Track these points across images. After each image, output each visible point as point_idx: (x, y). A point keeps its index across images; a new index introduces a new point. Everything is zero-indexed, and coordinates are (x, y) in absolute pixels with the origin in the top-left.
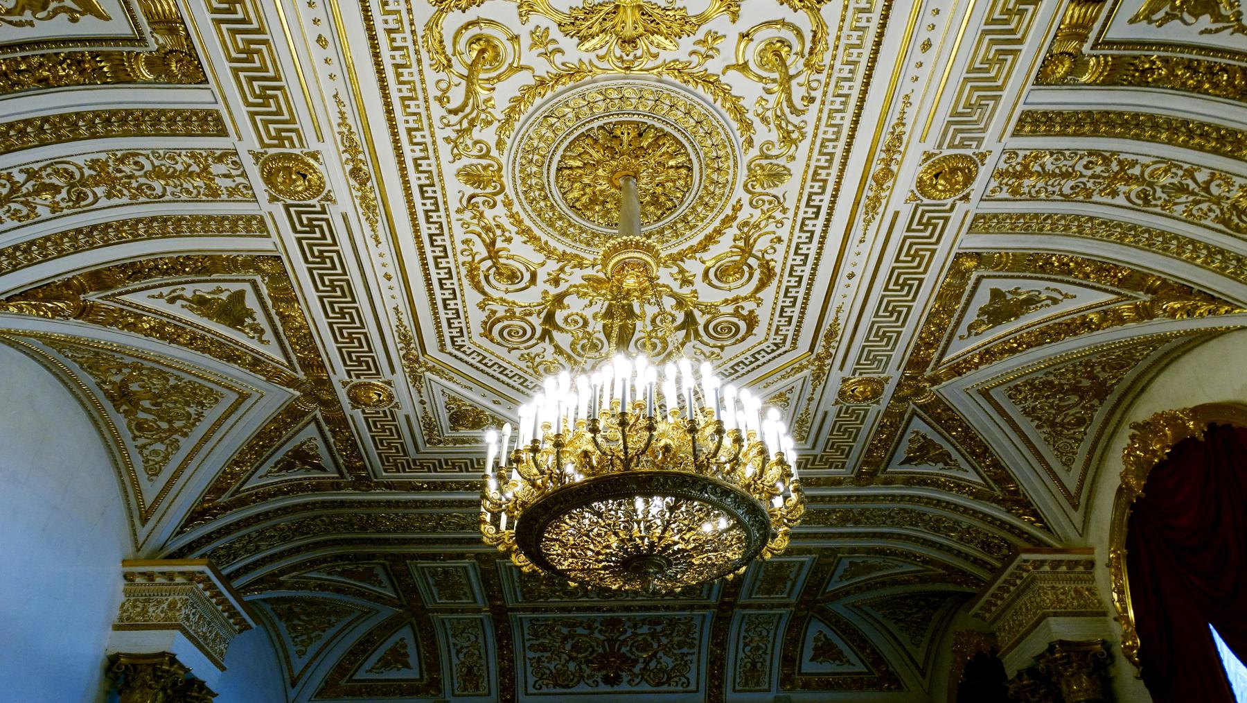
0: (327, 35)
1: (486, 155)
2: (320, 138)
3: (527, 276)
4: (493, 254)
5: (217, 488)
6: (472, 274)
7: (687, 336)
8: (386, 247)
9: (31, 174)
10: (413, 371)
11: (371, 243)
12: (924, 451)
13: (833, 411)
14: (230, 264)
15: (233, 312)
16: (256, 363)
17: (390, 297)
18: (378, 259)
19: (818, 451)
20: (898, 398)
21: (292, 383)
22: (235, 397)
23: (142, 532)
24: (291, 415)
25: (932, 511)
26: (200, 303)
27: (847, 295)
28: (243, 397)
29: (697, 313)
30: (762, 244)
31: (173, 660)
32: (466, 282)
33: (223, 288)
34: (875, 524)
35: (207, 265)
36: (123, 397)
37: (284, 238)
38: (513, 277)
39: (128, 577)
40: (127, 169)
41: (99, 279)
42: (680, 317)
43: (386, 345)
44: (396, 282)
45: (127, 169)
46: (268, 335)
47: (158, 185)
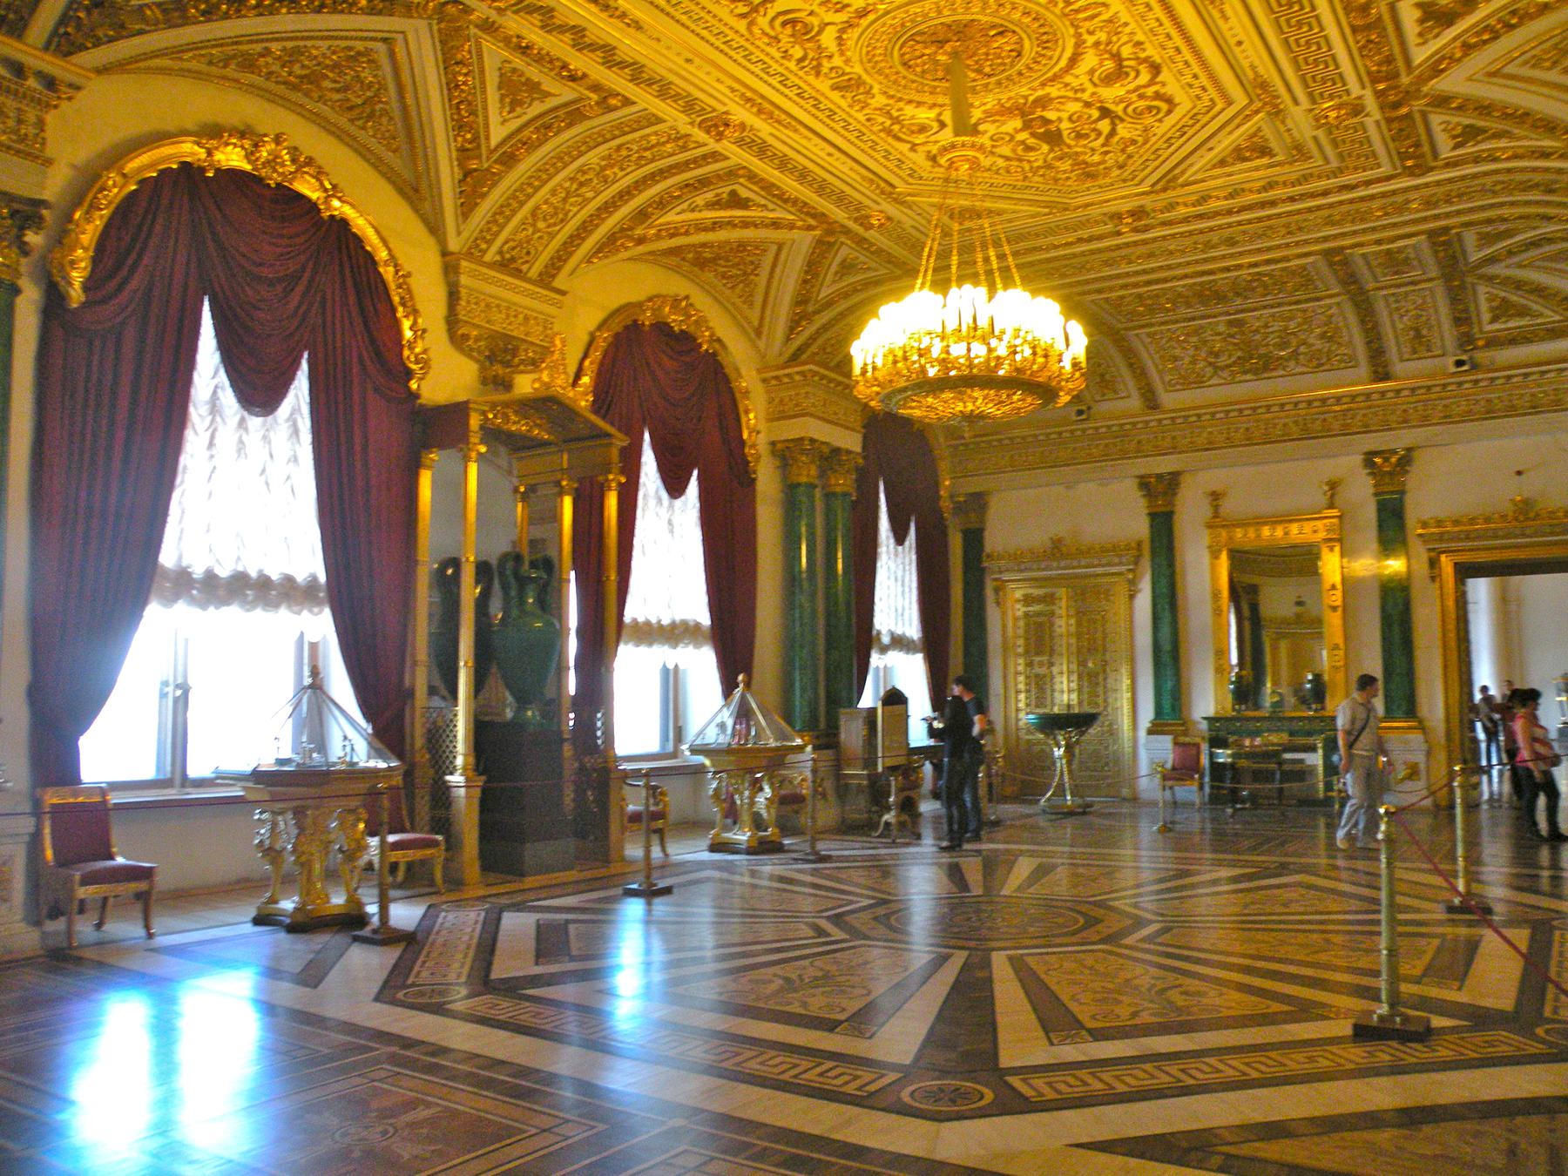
0: (690, 56)
1: (844, 74)
2: (724, 104)
3: (935, 125)
4: (896, 120)
5: (801, 300)
6: (889, 132)
7: (1114, 125)
8: (816, 140)
9: (572, 179)
10: (895, 200)
11: (804, 142)
12: (1471, 134)
13: (1320, 133)
14: (720, 177)
15: (736, 201)
16: (775, 224)
17: (843, 166)
18: (818, 149)
19: (1335, 164)
20: (1388, 105)
21: (810, 228)
22: (775, 247)
23: (762, 344)
24: (823, 248)
25: (1537, 178)
26: (711, 205)
27: (1252, 55)
28: (780, 246)
29: (1112, 107)
30: (1126, 51)
31: (812, 441)
32: (890, 140)
33: (725, 191)
34: (1471, 199)
35: (704, 182)
36: (701, 263)
37: (739, 157)
38: (923, 129)
39: (764, 381)
40: (624, 153)
41: (642, 215)
42: (1096, 114)
43: (861, 192)
44: (837, 154)
45: (624, 153)
46: (771, 206)
47: (648, 154)
